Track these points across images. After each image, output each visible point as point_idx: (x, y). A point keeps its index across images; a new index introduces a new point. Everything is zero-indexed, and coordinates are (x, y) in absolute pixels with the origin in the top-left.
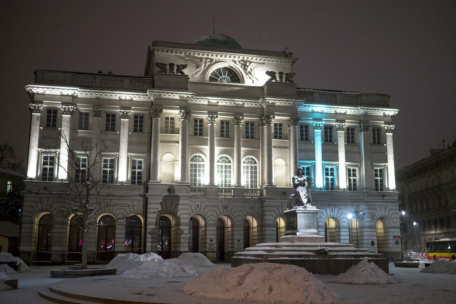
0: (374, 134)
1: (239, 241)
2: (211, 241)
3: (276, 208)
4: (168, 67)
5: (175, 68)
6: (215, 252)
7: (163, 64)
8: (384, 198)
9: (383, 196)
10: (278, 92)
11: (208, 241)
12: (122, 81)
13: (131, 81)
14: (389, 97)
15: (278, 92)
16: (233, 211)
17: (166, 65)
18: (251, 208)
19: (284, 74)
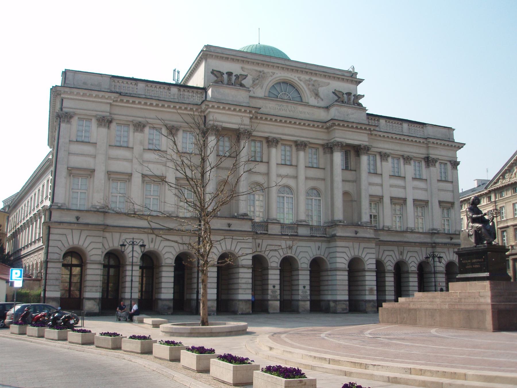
1: (304, 287)
2: (274, 287)
3: (348, 249)
4: (225, 76)
5: (234, 78)
6: (277, 300)
7: (220, 72)
8: (454, 241)
9: (451, 239)
10: (347, 115)
11: (270, 287)
12: (169, 89)
13: (179, 90)
14: (454, 130)
15: (347, 115)
16: (298, 251)
17: (223, 74)
18: (317, 249)
19: (352, 95)
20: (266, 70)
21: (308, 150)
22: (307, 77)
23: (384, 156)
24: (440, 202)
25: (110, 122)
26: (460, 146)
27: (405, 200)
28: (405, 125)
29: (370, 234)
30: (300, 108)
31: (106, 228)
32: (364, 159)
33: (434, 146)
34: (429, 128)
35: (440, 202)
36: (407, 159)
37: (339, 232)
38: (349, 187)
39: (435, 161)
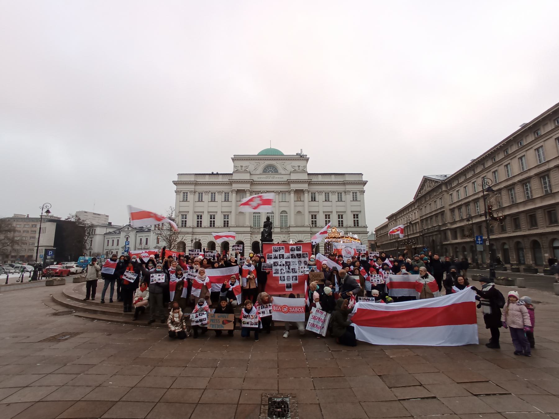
0: (353, 195)
20: (260, 162)
21: (281, 194)
22: (281, 162)
23: (320, 192)
24: (351, 212)
25: (195, 192)
26: (365, 183)
27: (332, 212)
28: (333, 176)
29: (309, 229)
30: (276, 176)
31: (193, 233)
32: (306, 195)
33: (351, 185)
34: (346, 175)
35: (351, 212)
36: (333, 192)
37: (291, 229)
38: (299, 209)
39: (349, 192)
